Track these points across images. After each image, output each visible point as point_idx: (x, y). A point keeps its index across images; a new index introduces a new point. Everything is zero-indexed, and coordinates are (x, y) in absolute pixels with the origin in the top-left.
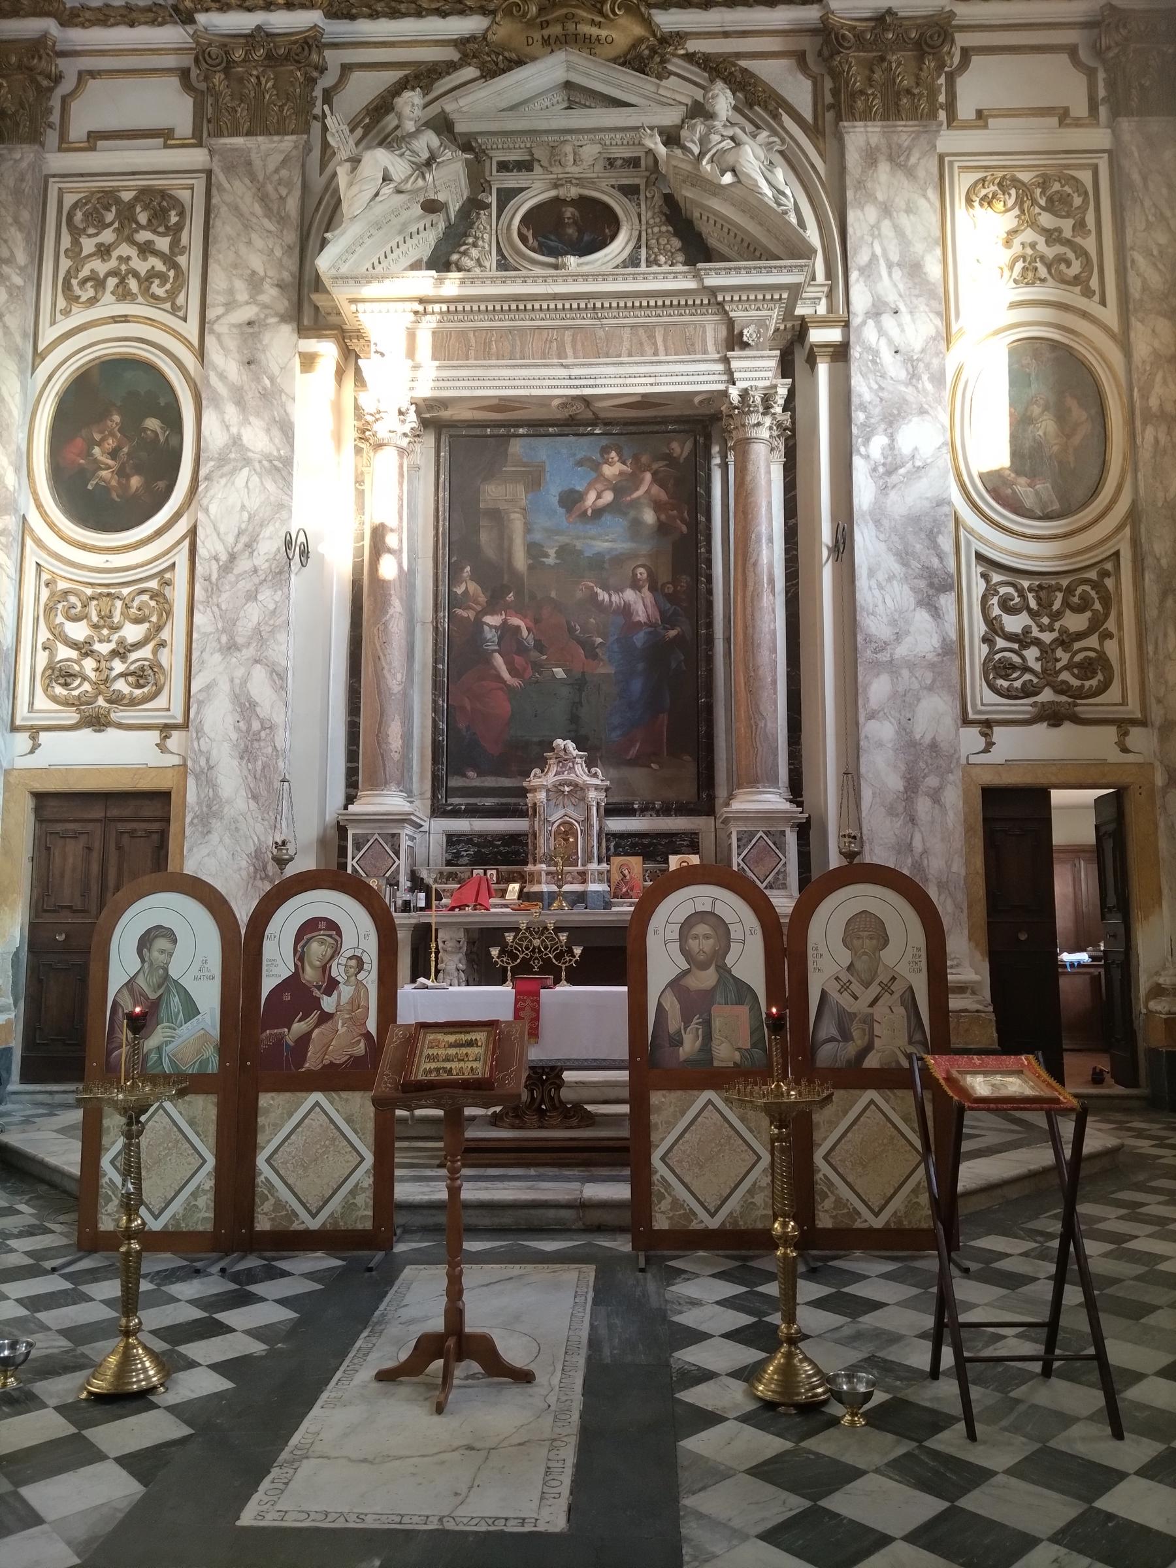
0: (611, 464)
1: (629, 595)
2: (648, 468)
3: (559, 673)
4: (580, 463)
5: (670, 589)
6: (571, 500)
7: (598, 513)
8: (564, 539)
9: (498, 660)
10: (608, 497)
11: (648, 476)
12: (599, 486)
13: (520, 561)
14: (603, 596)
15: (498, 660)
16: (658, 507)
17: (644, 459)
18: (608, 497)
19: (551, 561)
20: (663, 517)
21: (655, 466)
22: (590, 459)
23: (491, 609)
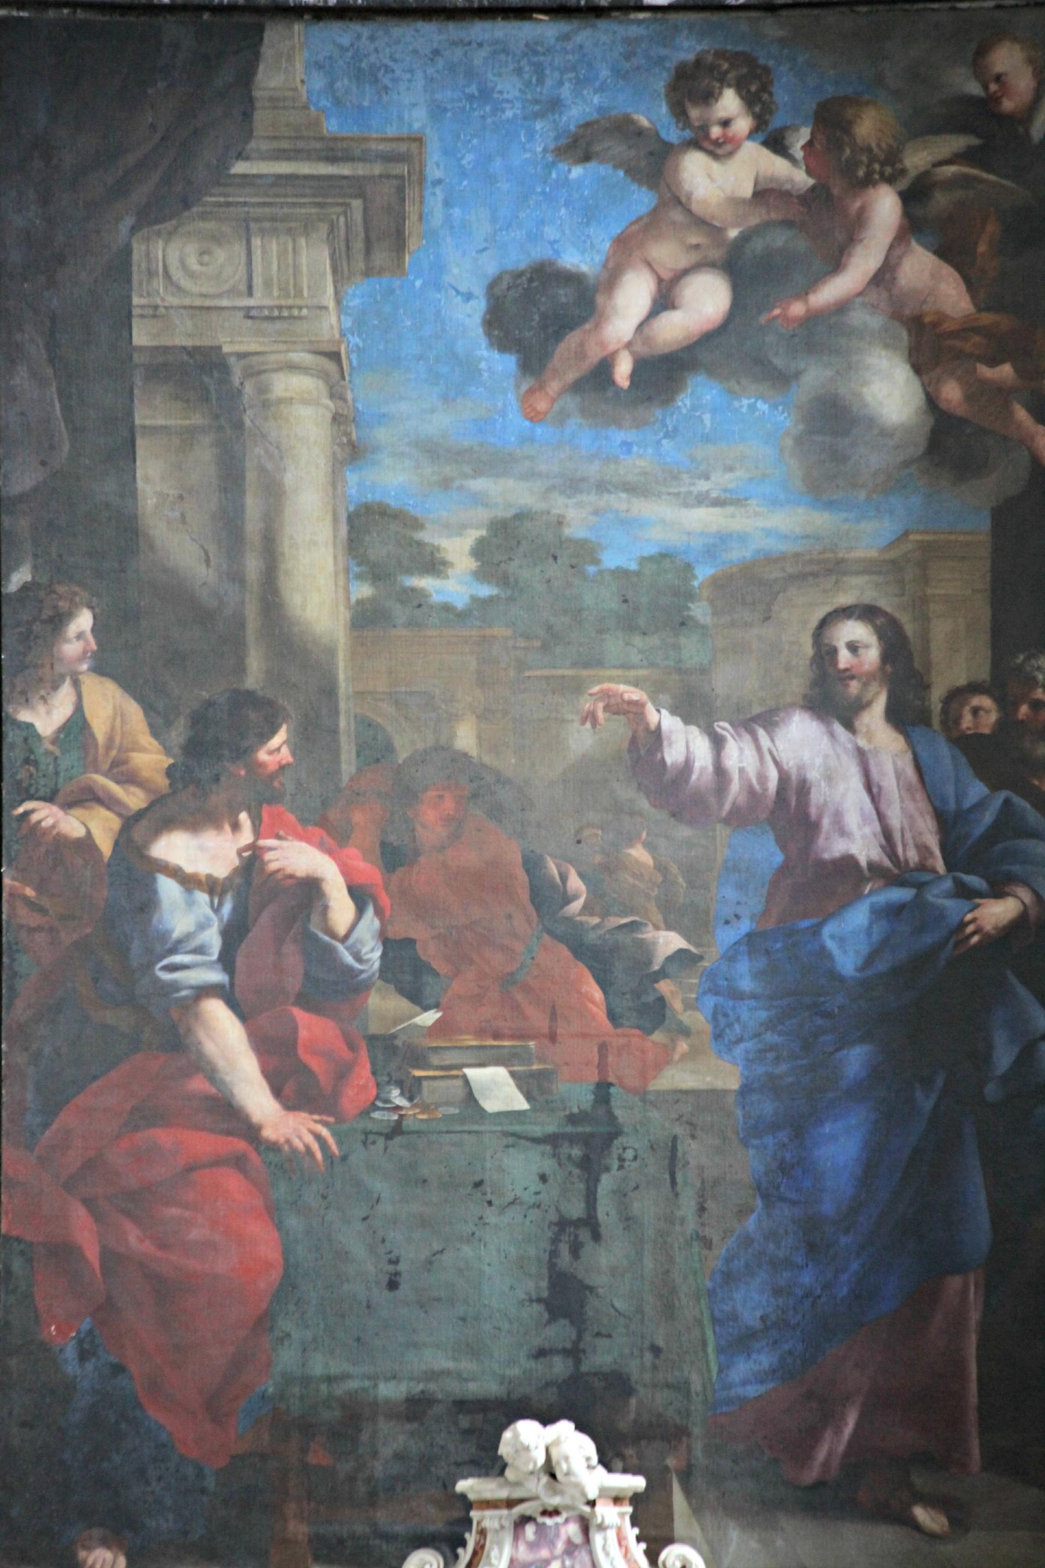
0: (719, 149)
1: (803, 741)
2: (886, 167)
3: (497, 1088)
4: (579, 147)
5: (983, 714)
6: (538, 313)
7: (663, 373)
8: (508, 493)
9: (224, 1035)
10: (707, 300)
11: (885, 206)
12: (667, 253)
13: (318, 590)
14: (684, 743)
15: (224, 1035)
16: (929, 345)
17: (868, 127)
18: (707, 300)
19: (456, 586)
20: (952, 393)
21: (917, 159)
22: (623, 128)
23: (187, 799)
